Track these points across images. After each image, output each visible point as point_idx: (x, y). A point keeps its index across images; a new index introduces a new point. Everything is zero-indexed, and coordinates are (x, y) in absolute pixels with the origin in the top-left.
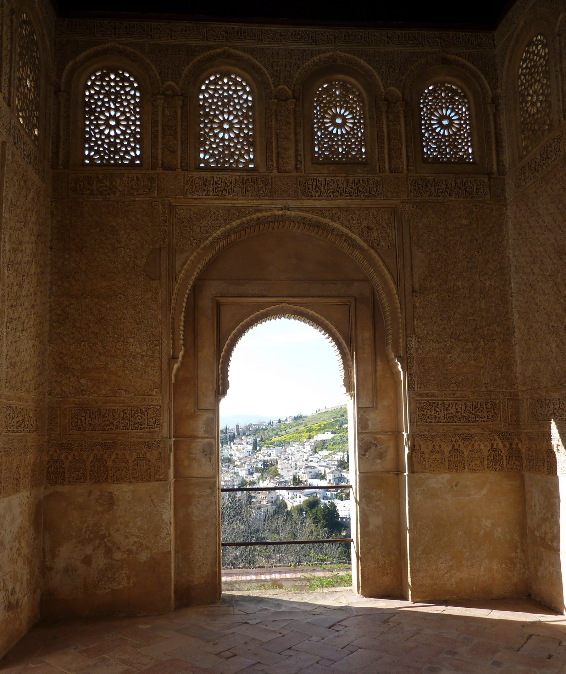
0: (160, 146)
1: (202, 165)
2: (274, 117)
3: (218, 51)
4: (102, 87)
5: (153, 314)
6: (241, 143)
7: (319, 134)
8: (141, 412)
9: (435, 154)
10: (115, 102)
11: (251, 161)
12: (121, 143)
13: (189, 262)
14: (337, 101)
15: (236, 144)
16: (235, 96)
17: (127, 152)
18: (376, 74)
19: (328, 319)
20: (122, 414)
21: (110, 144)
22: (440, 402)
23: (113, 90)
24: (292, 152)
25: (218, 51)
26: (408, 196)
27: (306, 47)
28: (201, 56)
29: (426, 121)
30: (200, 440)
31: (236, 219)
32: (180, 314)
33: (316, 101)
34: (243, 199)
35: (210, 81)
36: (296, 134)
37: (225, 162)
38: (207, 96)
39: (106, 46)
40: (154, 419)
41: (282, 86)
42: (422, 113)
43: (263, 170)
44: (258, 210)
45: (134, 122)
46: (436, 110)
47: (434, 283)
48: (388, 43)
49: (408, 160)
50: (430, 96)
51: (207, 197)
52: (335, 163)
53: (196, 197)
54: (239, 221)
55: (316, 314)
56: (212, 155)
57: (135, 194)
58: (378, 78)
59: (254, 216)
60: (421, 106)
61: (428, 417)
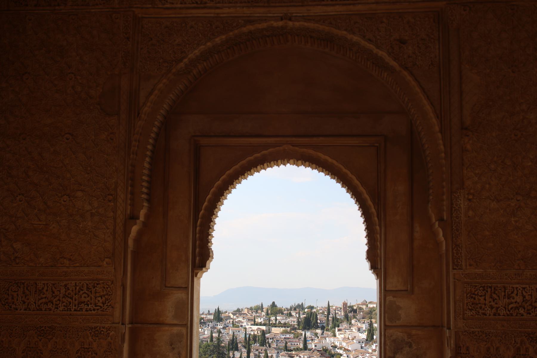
8: (88, 288)
20: (63, 291)
22: (499, 285)
30: (167, 328)
34: (229, 8)
40: (104, 298)
51: (183, 6)
53: (168, 6)
54: (224, 37)
55: (330, 160)
59: (245, 29)
61: (481, 308)
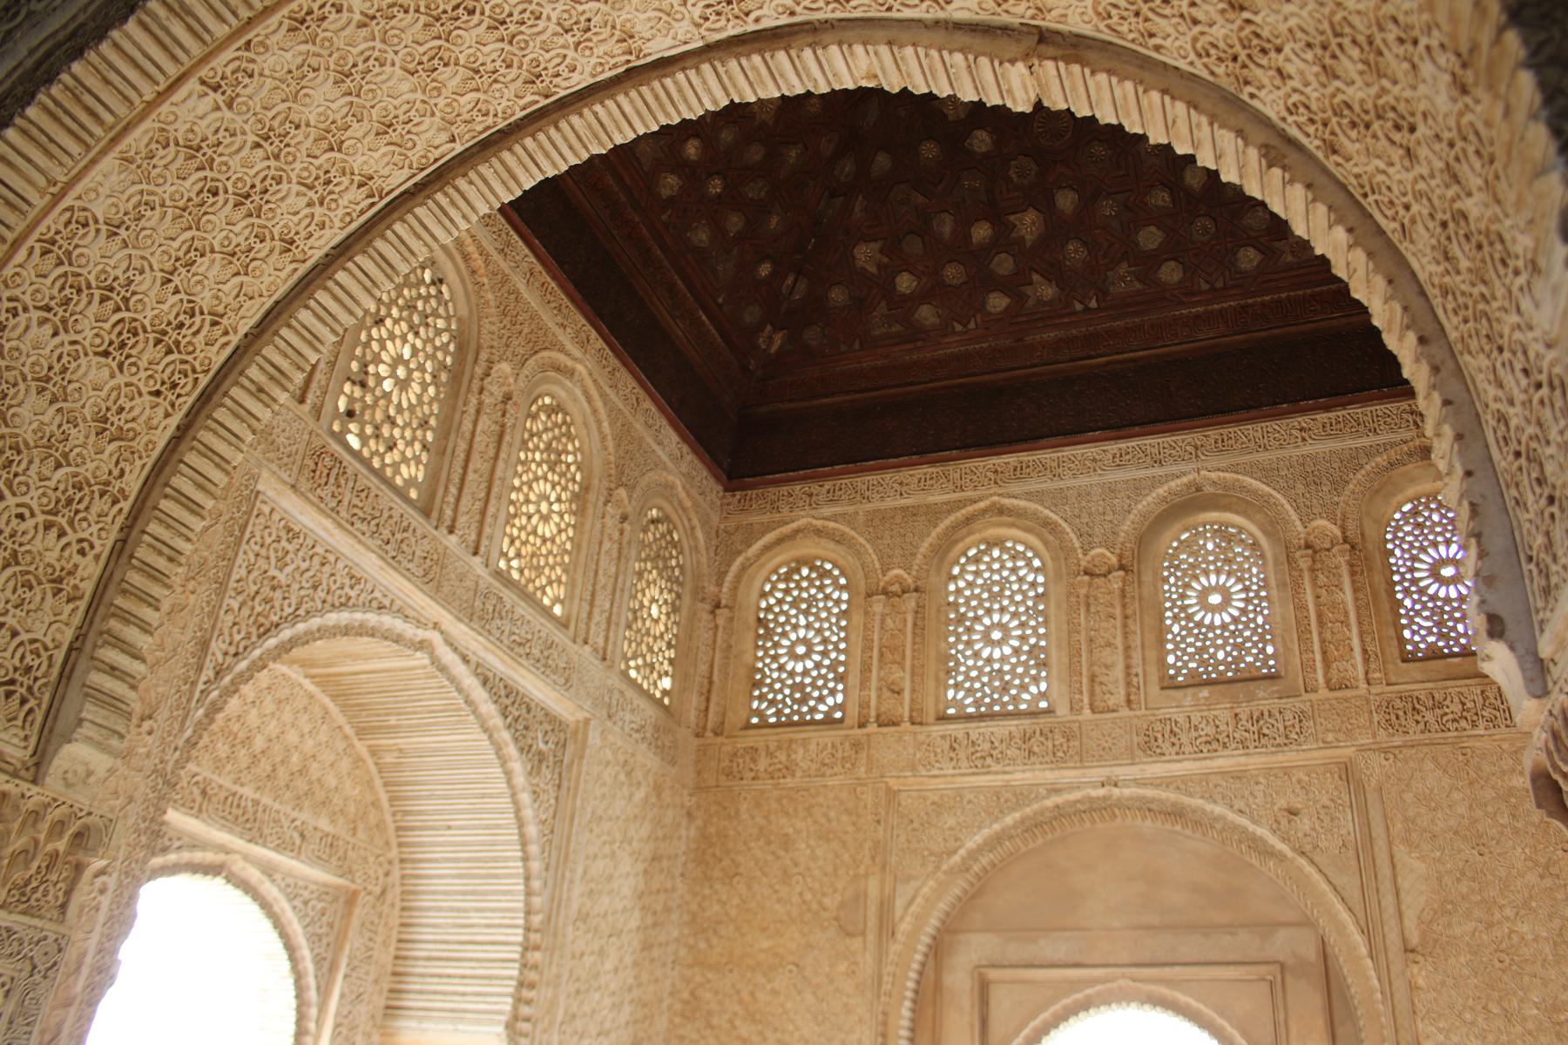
0: (874, 683)
1: (951, 711)
2: (1083, 610)
3: (982, 505)
4: (787, 591)
5: (846, 1005)
6: (1025, 664)
7: (1176, 629)
9: (1431, 639)
10: (806, 613)
11: (1043, 695)
12: (813, 685)
13: (919, 900)
14: (1208, 563)
15: (1014, 667)
16: (1013, 578)
17: (821, 699)
18: (1284, 501)
19: (1222, 1015)
21: (793, 687)
23: (805, 595)
24: (1118, 672)
25: (982, 505)
26: (1374, 736)
27: (1141, 474)
28: (952, 518)
29: (1402, 574)
31: (1014, 809)
32: (901, 1004)
33: (1168, 568)
35: (968, 559)
36: (1126, 635)
37: (994, 702)
38: (962, 584)
39: (794, 525)
41: (1098, 550)
42: (1392, 561)
43: (1062, 711)
44: (1054, 790)
45: (836, 644)
46: (1423, 549)
47: (1458, 931)
48: (1304, 439)
49: (1366, 660)
50: (1407, 523)
52: (1210, 683)
53: (935, 772)
54: (1017, 815)
55: (1194, 1004)
56: (970, 691)
57: (828, 772)
58: (1287, 506)
59: (1049, 803)
60: (1390, 546)
